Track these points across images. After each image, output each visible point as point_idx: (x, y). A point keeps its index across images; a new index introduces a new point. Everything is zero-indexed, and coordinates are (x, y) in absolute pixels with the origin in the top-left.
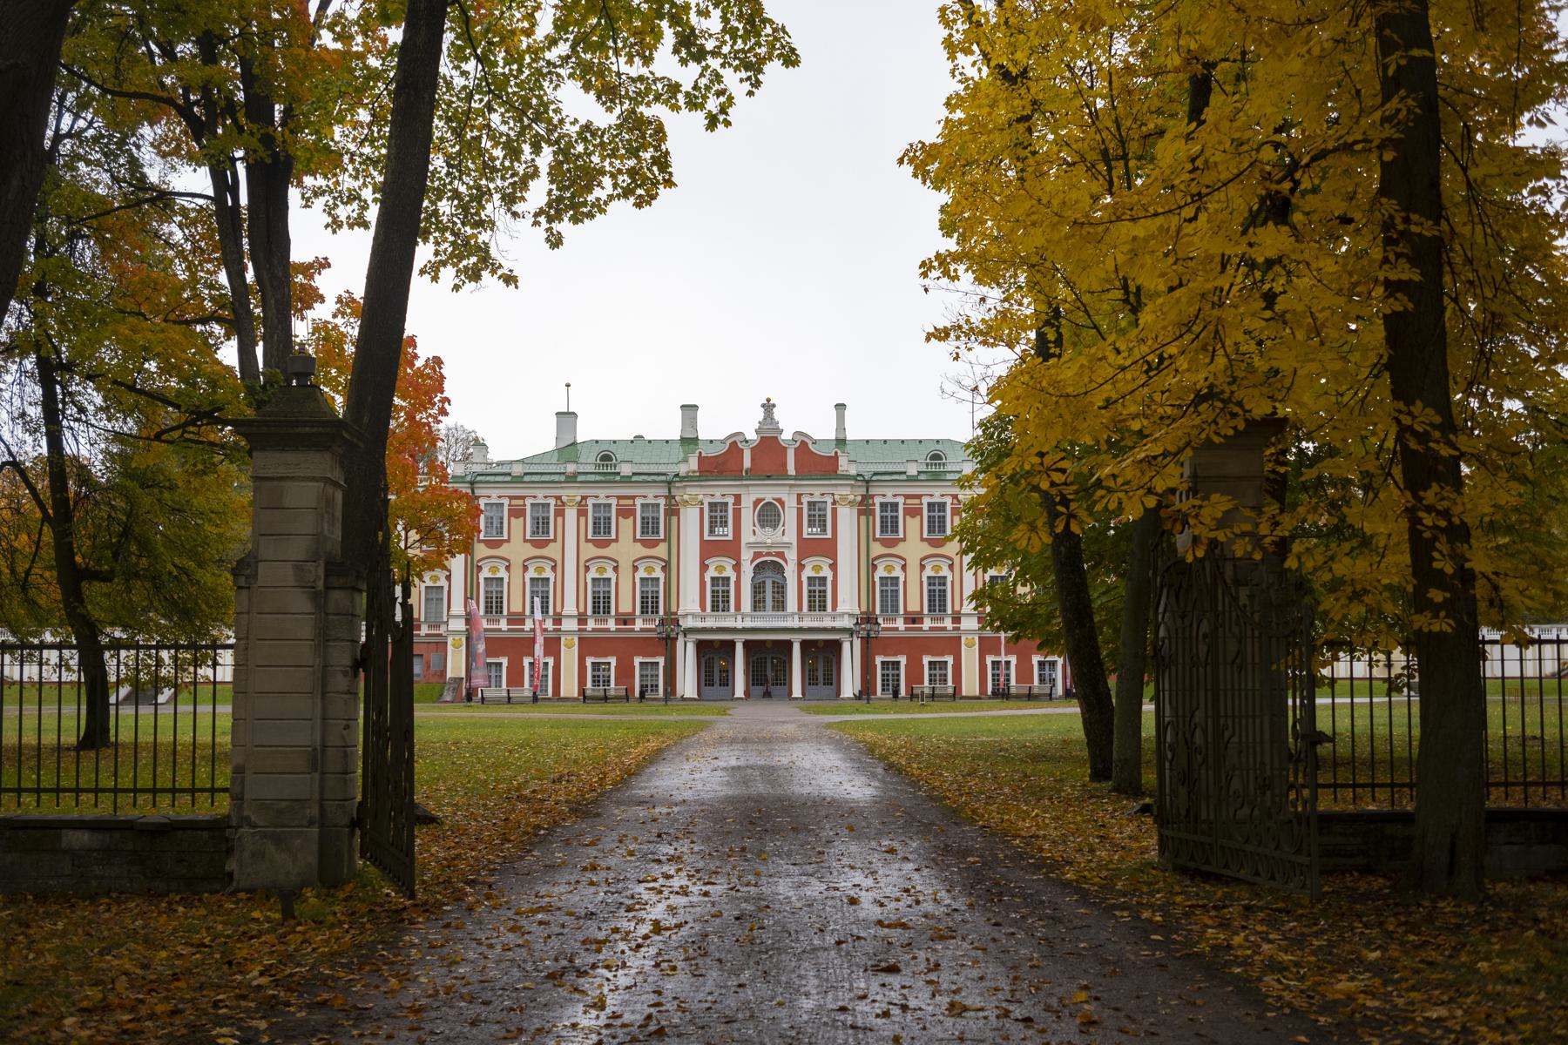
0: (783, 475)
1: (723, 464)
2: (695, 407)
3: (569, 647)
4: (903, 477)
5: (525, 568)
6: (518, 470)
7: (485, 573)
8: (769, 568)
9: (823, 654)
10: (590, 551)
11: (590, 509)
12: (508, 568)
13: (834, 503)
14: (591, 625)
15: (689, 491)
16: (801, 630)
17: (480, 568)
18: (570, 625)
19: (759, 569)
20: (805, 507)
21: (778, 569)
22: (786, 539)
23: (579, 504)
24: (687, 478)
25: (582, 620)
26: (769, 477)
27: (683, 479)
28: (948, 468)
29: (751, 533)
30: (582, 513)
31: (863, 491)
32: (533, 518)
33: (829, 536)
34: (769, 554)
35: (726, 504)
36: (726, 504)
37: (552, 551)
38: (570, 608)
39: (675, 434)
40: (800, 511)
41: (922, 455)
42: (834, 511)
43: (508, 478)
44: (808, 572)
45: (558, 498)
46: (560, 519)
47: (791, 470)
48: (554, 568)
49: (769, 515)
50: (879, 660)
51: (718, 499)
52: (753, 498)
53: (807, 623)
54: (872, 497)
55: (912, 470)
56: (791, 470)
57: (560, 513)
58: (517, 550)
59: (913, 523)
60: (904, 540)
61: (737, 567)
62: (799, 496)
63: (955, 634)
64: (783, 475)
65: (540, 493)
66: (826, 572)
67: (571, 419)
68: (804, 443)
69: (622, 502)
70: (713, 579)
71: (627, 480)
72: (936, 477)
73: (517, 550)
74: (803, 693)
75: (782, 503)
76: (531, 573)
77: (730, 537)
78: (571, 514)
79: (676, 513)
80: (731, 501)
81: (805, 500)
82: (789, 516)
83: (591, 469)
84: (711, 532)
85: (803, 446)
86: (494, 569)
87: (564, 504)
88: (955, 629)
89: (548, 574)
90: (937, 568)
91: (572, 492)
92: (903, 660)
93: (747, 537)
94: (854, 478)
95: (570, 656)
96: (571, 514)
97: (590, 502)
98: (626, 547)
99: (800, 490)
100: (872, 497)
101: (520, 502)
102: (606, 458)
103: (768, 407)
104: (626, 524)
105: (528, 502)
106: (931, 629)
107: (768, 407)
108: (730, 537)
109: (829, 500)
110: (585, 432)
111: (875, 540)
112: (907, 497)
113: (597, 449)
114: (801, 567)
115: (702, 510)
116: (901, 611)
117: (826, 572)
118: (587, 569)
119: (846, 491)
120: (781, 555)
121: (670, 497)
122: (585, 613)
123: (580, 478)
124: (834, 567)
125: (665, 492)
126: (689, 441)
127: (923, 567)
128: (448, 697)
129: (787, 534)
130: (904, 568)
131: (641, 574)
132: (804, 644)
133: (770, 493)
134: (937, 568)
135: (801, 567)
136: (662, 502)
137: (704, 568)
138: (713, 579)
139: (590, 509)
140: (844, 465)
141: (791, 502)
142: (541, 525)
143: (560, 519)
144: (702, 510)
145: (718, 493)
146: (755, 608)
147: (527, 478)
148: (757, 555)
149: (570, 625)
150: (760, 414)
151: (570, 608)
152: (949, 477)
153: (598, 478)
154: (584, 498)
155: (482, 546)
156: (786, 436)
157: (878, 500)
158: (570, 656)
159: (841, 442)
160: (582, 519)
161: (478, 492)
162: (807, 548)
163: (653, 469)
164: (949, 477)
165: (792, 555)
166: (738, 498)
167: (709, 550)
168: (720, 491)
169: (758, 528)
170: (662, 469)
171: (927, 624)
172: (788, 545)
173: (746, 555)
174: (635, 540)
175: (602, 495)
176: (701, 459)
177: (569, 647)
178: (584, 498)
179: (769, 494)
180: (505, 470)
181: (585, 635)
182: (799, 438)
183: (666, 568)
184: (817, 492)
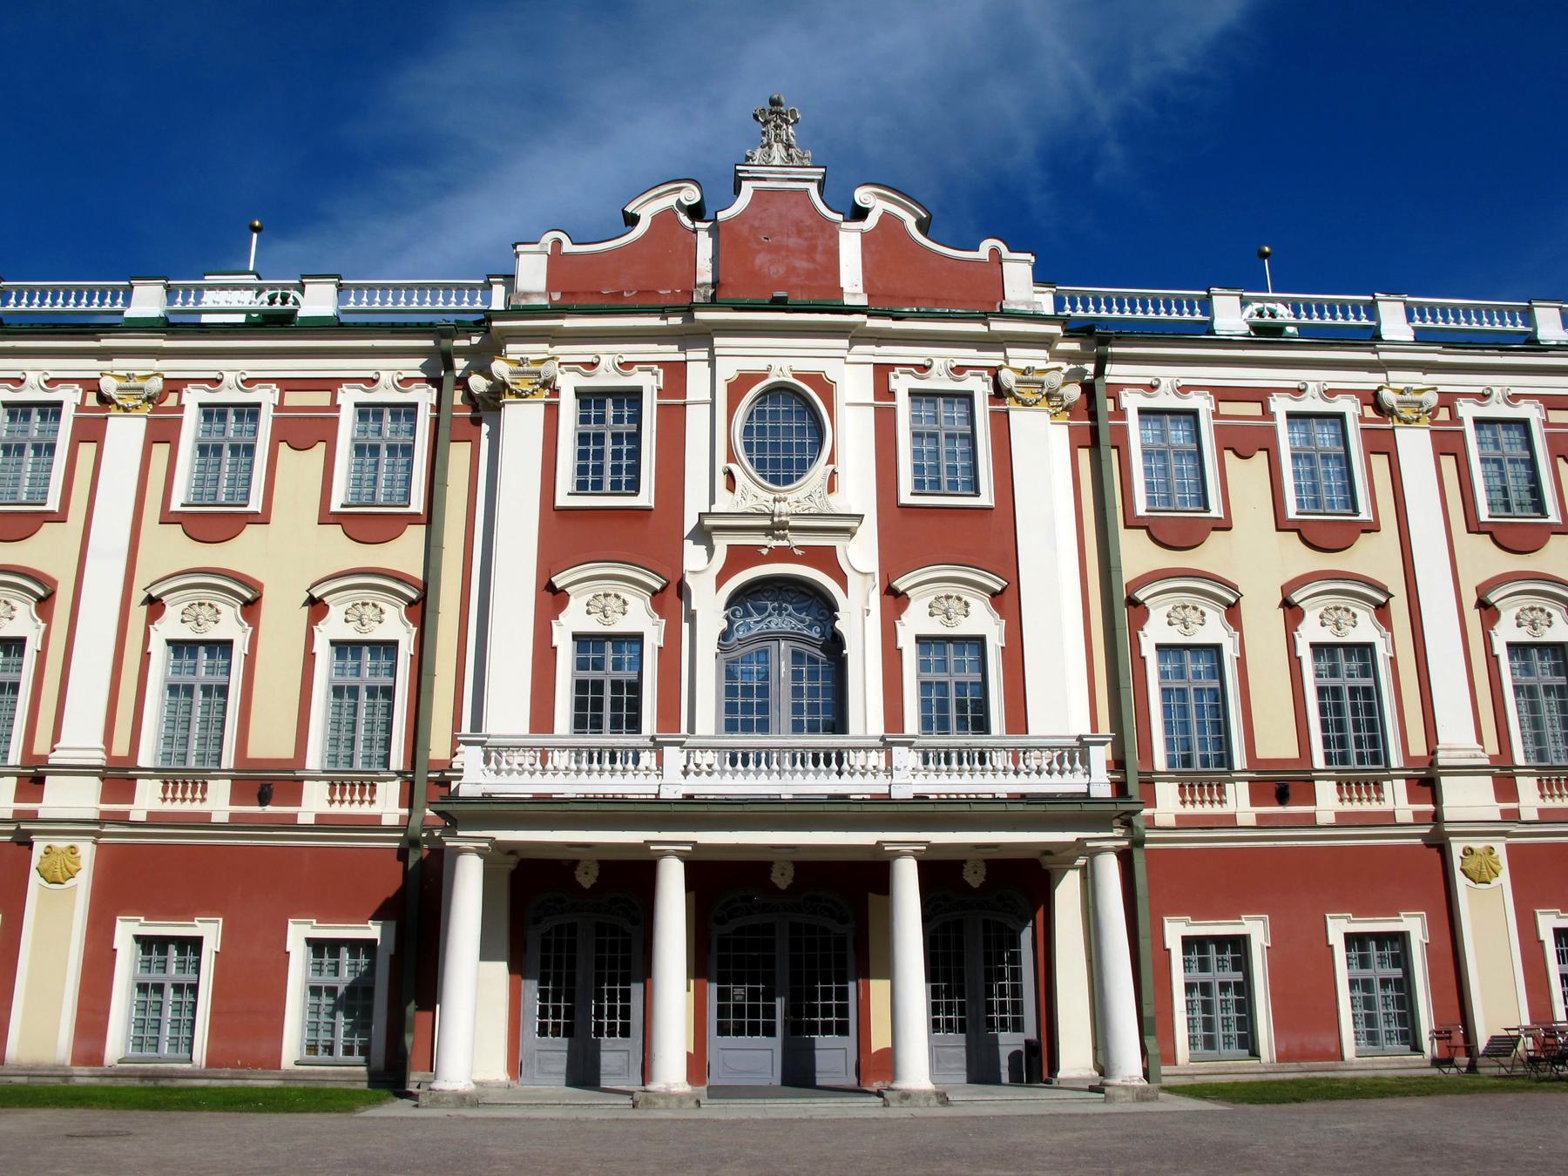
8: (784, 599)
9: (990, 914)
10: (171, 550)
11: (191, 423)
14: (148, 798)
20: (903, 405)
22: (838, 503)
25: (118, 778)
30: (163, 431)
42: (1001, 424)
44: (916, 621)
45: (90, 385)
49: (787, 427)
50: (1175, 931)
52: (728, 369)
54: (1114, 391)
59: (1249, 476)
60: (1224, 525)
62: (882, 371)
66: (981, 620)
69: (293, 399)
70: (580, 639)
75: (826, 388)
77: (645, 498)
78: (125, 434)
80: (649, 383)
81: (902, 384)
82: (851, 432)
87: (104, 400)
92: (1256, 929)
97: (193, 398)
98: (291, 547)
100: (1114, 391)
106: (1344, 820)
109: (980, 388)
111: (1132, 523)
112: (1223, 394)
114: (894, 600)
115: (552, 410)
116: (1239, 761)
117: (981, 620)
118: (155, 605)
120: (826, 559)
124: (1006, 601)
127: (1292, 612)
130: (1233, 613)
131: (335, 626)
133: (782, 359)
135: (894, 600)
137: (552, 598)
138: (580, 639)
143: (87, 451)
148: (739, 558)
154: (175, 385)
157: (1132, 402)
160: (161, 452)
162: (912, 537)
165: (861, 553)
166: (675, 374)
167: (567, 537)
171: (1328, 801)
174: (327, 517)
179: (782, 359)
183: (421, 609)
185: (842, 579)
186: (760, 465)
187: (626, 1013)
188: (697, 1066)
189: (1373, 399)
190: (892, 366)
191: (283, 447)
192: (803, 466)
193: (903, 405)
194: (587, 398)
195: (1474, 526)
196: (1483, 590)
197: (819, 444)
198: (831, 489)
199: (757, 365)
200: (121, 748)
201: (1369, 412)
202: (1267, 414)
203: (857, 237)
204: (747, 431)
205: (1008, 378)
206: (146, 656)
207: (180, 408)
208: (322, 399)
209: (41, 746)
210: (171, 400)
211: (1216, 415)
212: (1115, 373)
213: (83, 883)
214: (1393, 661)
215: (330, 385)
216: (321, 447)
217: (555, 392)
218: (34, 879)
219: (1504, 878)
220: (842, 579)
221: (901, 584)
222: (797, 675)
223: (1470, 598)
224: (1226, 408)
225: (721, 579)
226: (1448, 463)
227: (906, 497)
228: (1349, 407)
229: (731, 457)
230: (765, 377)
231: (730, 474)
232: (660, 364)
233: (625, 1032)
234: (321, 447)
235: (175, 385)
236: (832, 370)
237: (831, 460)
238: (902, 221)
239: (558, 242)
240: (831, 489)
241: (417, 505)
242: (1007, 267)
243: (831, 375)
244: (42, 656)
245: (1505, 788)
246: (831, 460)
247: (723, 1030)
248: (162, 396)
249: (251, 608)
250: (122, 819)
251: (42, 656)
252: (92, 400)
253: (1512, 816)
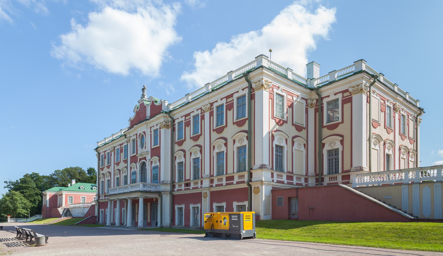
10: (215, 135)
14: (216, 182)
30: (211, 114)
46: (203, 121)
57: (203, 118)
122: (213, 176)
139: (215, 110)
149: (206, 183)
154: (212, 104)
181: (213, 189)
191: (228, 111)
210: (212, 108)
213: (208, 198)
218: (203, 198)
235: (212, 104)
241: (247, 117)
244: (201, 160)
248: (211, 107)
249: (226, 145)
251: (201, 160)
252: (203, 112)
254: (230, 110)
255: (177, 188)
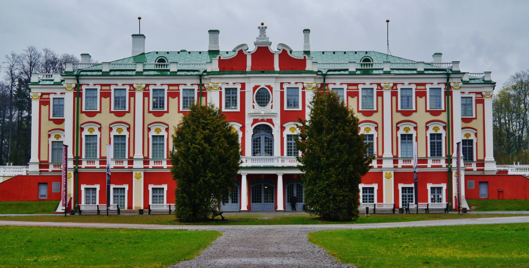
0: (271, 70)
1: (233, 65)
2: (217, 31)
3: (138, 178)
4: (347, 72)
5: (111, 129)
6: (106, 69)
7: (86, 132)
10: (151, 118)
12: (100, 129)
13: (304, 88)
15: (213, 81)
16: (283, 168)
17: (82, 129)
18: (138, 164)
19: (256, 130)
21: (269, 130)
22: (273, 111)
23: (144, 89)
24: (213, 73)
25: (146, 161)
26: (263, 72)
27: (209, 74)
28: (374, 67)
29: (252, 108)
30: (146, 95)
31: (322, 81)
32: (115, 98)
33: (300, 109)
34: (263, 120)
35: (236, 89)
36: (236, 89)
37: (127, 118)
38: (139, 154)
39: (206, 48)
40: (282, 94)
41: (358, 59)
42: (304, 94)
43: (100, 73)
45: (131, 85)
46: (132, 99)
47: (277, 68)
48: (128, 129)
51: (231, 86)
53: (287, 164)
54: (327, 85)
55: (352, 68)
56: (277, 68)
57: (132, 95)
58: (106, 118)
61: (243, 129)
62: (282, 84)
63: (379, 170)
64: (271, 70)
65: (120, 83)
67: (142, 39)
68: (284, 51)
71: (174, 74)
72: (366, 72)
73: (106, 118)
74: (284, 207)
75: (271, 89)
76: (114, 133)
78: (139, 95)
79: (205, 95)
80: (239, 87)
81: (285, 86)
82: (275, 97)
83: (152, 67)
84: (227, 106)
85: (284, 55)
86: (91, 130)
87: (135, 89)
88: (379, 167)
89: (125, 133)
90: (407, 129)
91: (139, 82)
93: (249, 110)
94: (316, 73)
95: (138, 184)
96: (139, 95)
97: (151, 88)
99: (283, 81)
101: (108, 88)
102: (162, 60)
103: (263, 29)
104: (174, 102)
105: (113, 88)
107: (263, 29)
108: (238, 110)
109: (300, 86)
110: (153, 45)
113: (157, 56)
114: (283, 129)
115: (221, 93)
118: (149, 130)
119: (311, 81)
120: (270, 121)
121: (201, 85)
123: (145, 73)
125: (198, 82)
126: (213, 53)
128: (61, 208)
129: (273, 109)
132: (285, 176)
133: (262, 81)
134: (436, 129)
135: (283, 129)
136: (196, 88)
140: (309, 67)
141: (276, 88)
142: (120, 101)
143: (132, 99)
144: (221, 93)
145: (231, 82)
146: (254, 154)
147: (112, 73)
148: (255, 121)
149: (138, 164)
150: (257, 33)
151: (139, 154)
152: (375, 72)
153: (156, 73)
154: (147, 85)
155: (84, 115)
156: (273, 48)
158: (138, 184)
159: (307, 53)
160: (146, 99)
161: (81, 82)
163: (191, 67)
164: (375, 72)
166: (243, 86)
168: (232, 81)
169: (256, 105)
170: (196, 67)
172: (274, 115)
173: (248, 121)
174: (179, 112)
175: (159, 83)
176: (221, 62)
177: (138, 178)
178: (147, 85)
180: (99, 68)
181: (148, 171)
182: (282, 48)
184: (293, 81)
185: (273, 125)
186: (259, 103)
187: (237, 199)
188: (249, 207)
189: (379, 85)
190: (283, 83)
192: (267, 103)
193: (285, 91)
194: (227, 89)
195: (397, 111)
196: (397, 124)
197: (269, 100)
198: (272, 108)
199: (257, 84)
200: (146, 155)
201: (379, 88)
202: (358, 89)
203: (278, 56)
204: (256, 96)
205: (305, 85)
206: (148, 139)
207: (149, 90)
208: (176, 88)
209: (131, 155)
210: (147, 88)
211: (347, 89)
212: (327, 81)
214: (377, 138)
215: (178, 85)
216: (177, 98)
217: (221, 89)
218: (134, 179)
219: (393, 178)
220: (273, 125)
221: (284, 125)
222: (266, 141)
223: (394, 125)
224: (350, 87)
225: (252, 125)
226: (394, 98)
227: (285, 109)
228: (375, 87)
229: (254, 102)
230: (259, 86)
231: (253, 106)
232: (241, 83)
233: (237, 202)
234: (177, 98)
236: (272, 85)
237: (272, 102)
238: (286, 51)
239: (220, 57)
240: (272, 108)
242: (307, 61)
243: (272, 86)
244: (129, 139)
245: (396, 162)
246: (272, 102)
247: (253, 202)
250: (148, 168)
252: (132, 88)
253: (396, 167)
254: (173, 97)
255: (84, 164)
